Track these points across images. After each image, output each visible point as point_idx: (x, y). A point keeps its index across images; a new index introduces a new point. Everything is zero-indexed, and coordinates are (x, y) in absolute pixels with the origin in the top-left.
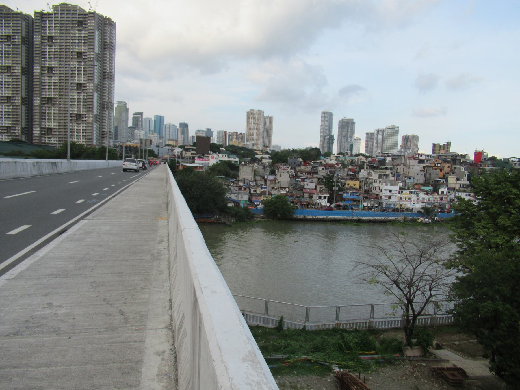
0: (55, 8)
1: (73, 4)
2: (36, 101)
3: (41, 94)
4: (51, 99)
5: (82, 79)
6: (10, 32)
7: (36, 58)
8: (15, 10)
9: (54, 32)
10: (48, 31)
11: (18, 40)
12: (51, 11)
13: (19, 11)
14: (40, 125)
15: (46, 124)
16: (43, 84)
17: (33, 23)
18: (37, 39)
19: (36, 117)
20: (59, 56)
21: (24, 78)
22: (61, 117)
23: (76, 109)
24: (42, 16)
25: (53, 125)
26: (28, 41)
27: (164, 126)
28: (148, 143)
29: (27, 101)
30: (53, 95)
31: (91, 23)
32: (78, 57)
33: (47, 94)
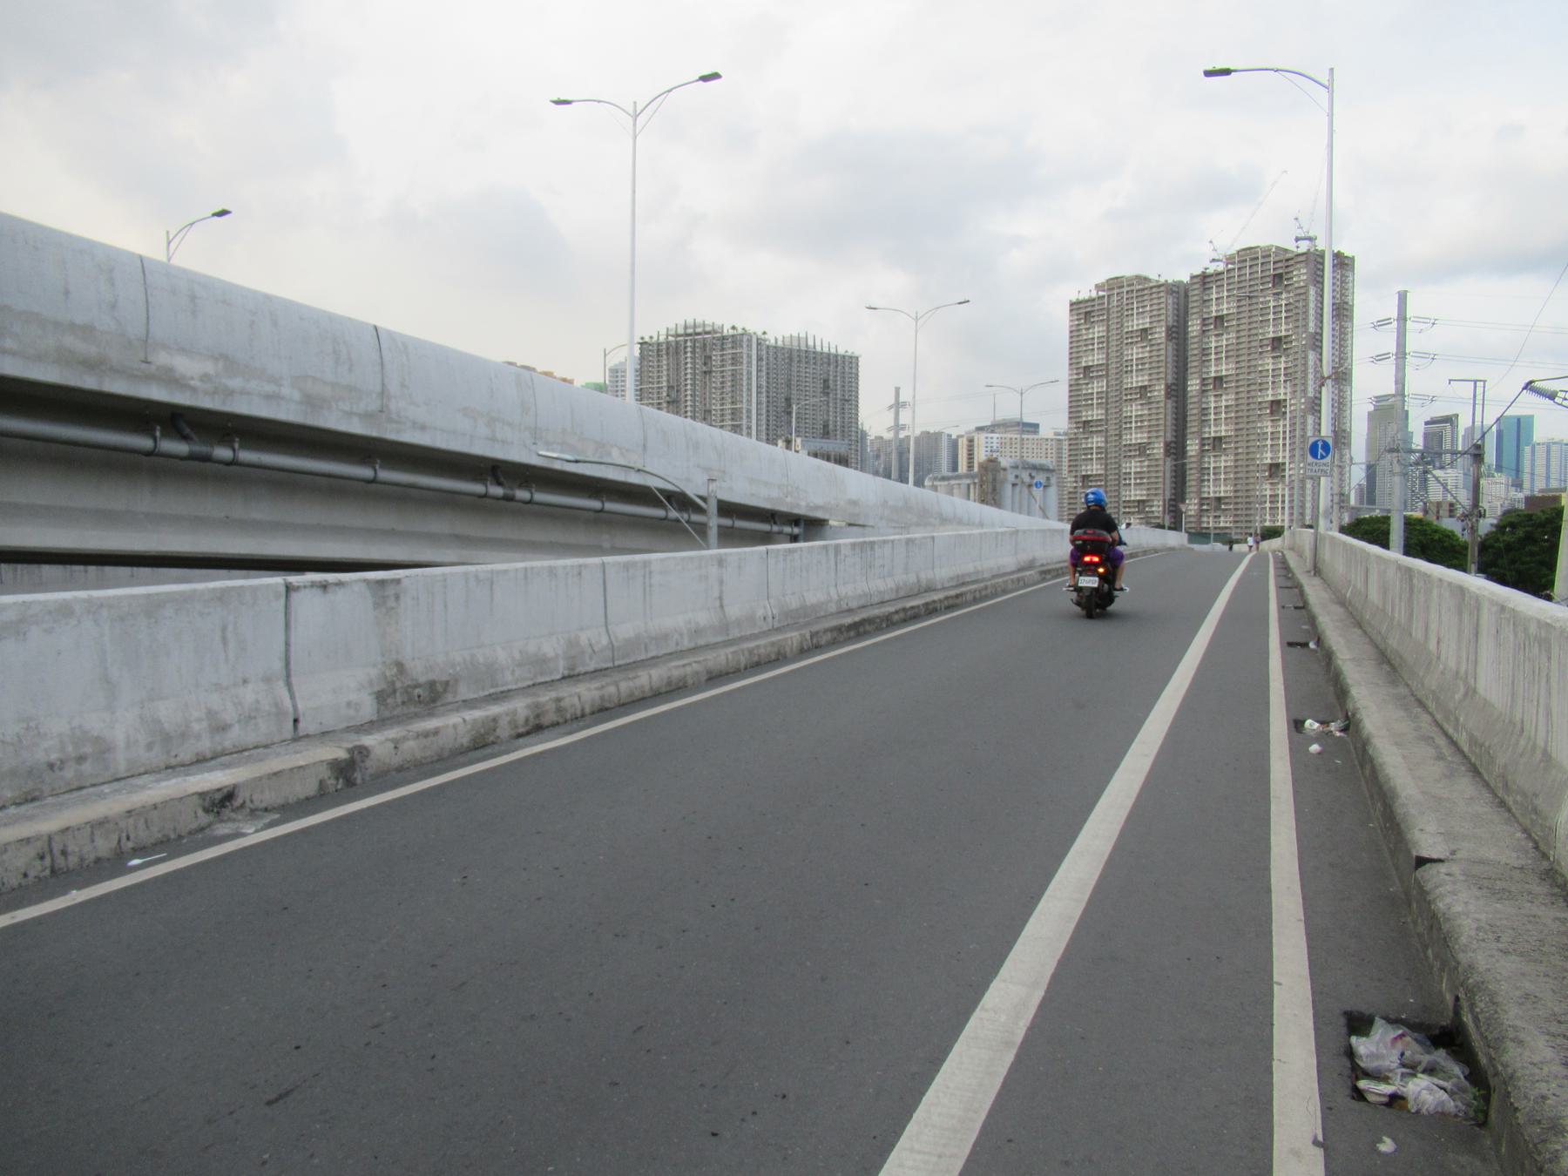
0: (1230, 260)
1: (1262, 244)
2: (1193, 447)
3: (1200, 432)
4: (1220, 439)
5: (1282, 391)
6: (1145, 322)
7: (1193, 363)
8: (1153, 276)
9: (1225, 309)
10: (1214, 308)
11: (1160, 334)
12: (1221, 267)
13: (1162, 280)
14: (1200, 492)
15: (1211, 490)
16: (1204, 411)
17: (1186, 296)
18: (1194, 327)
19: (1192, 477)
20: (1233, 353)
21: (1170, 404)
22: (1241, 473)
23: (1269, 455)
24: (1204, 280)
25: (1224, 490)
26: (1177, 333)
27: (1527, 449)
28: (1444, 512)
29: (1176, 449)
30: (1223, 430)
31: (1300, 275)
32: (1273, 349)
33: (1212, 431)
